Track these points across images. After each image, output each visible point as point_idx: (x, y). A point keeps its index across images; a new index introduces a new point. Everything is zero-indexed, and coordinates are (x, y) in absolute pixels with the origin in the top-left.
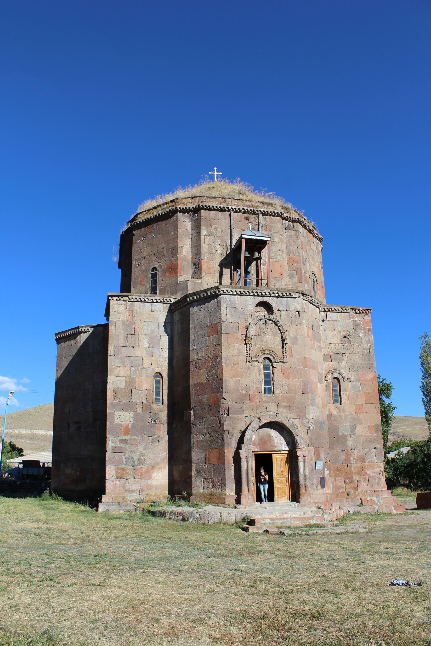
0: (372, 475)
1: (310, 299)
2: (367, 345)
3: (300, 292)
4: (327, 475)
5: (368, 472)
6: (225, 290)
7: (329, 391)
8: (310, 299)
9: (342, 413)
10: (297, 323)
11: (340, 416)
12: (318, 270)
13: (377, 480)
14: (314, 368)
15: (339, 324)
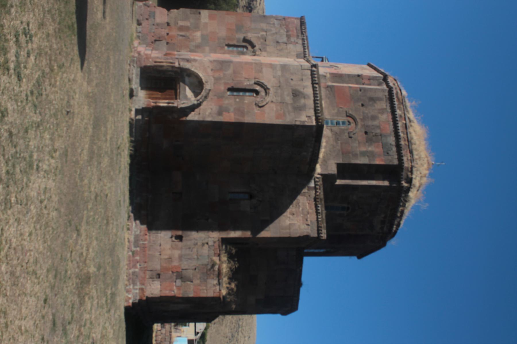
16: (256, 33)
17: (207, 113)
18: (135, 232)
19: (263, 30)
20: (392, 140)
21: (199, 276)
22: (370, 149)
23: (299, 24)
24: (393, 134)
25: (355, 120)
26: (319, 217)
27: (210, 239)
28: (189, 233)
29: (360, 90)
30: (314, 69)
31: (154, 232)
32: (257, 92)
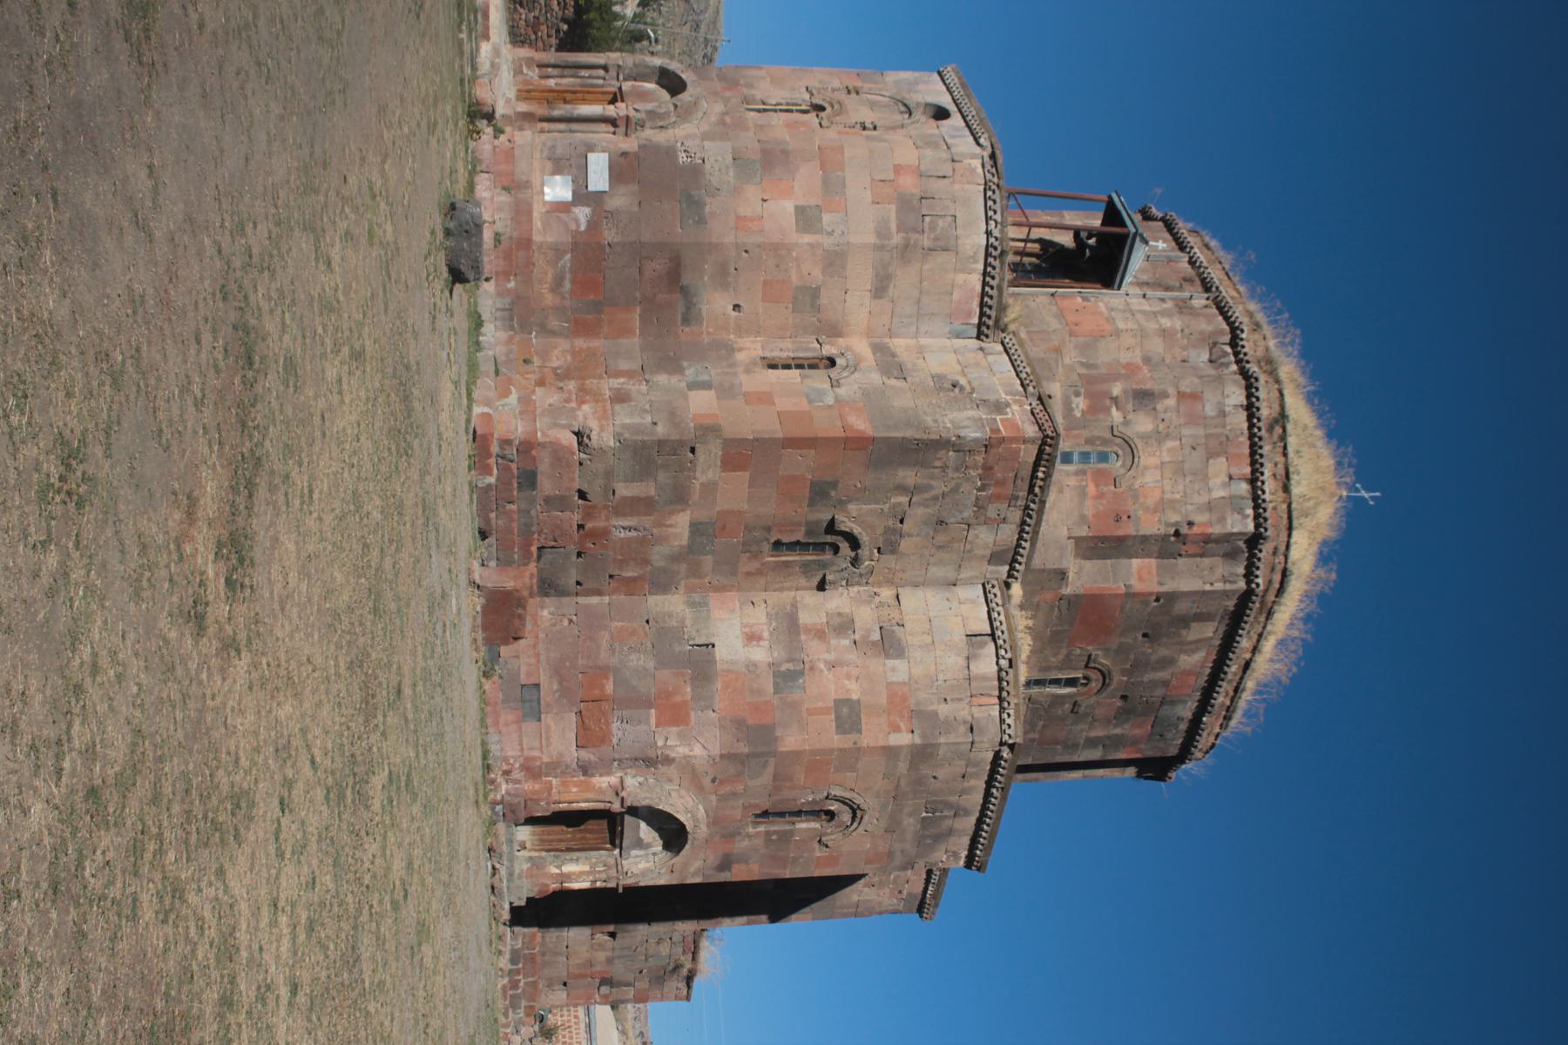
0: (579, 413)
1: (994, 187)
2: (946, 420)
3: (996, 146)
4: (577, 221)
5: (586, 407)
6: (949, 69)
7: (794, 351)
8: (994, 187)
9: (741, 369)
10: (919, 143)
11: (733, 365)
12: (1157, 493)
13: (564, 422)
14: (826, 183)
15: (986, 375)
16: (876, 503)
17: (692, 870)
18: (512, 945)
19: (902, 489)
20: (1187, 710)
21: (647, 979)
22: (1118, 731)
23: (1032, 459)
24: (1198, 695)
25: (1105, 675)
26: (930, 888)
27: (676, 933)
28: (631, 927)
29: (1157, 600)
30: (1006, 753)
31: (552, 930)
32: (831, 815)
